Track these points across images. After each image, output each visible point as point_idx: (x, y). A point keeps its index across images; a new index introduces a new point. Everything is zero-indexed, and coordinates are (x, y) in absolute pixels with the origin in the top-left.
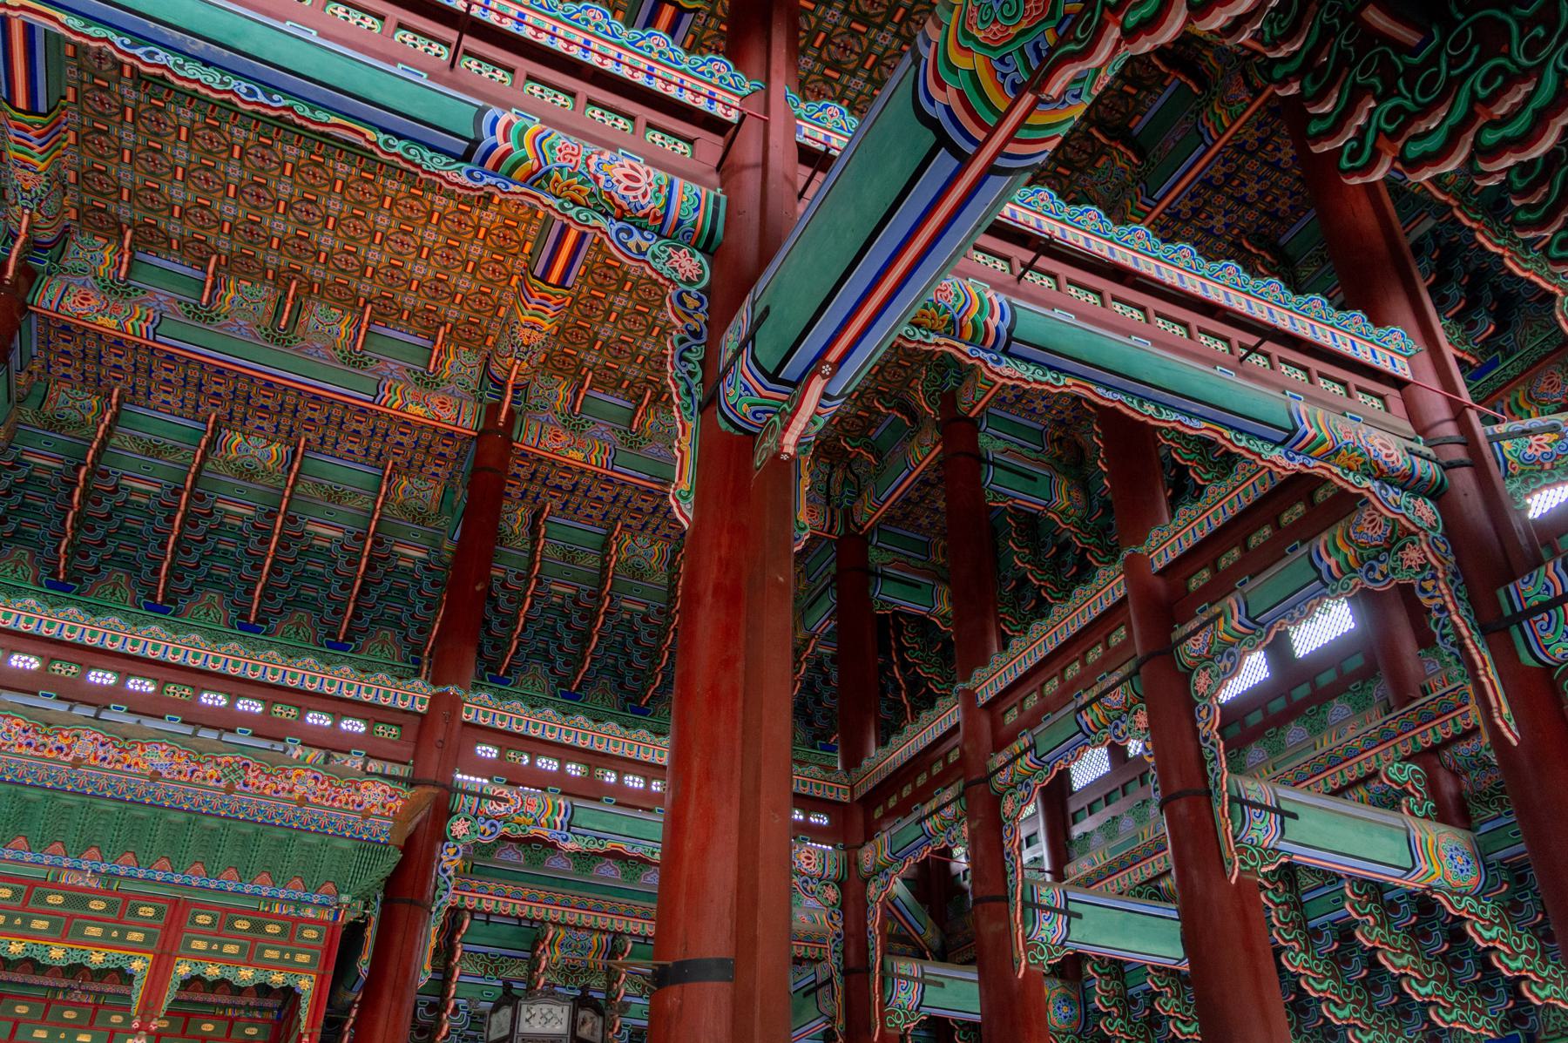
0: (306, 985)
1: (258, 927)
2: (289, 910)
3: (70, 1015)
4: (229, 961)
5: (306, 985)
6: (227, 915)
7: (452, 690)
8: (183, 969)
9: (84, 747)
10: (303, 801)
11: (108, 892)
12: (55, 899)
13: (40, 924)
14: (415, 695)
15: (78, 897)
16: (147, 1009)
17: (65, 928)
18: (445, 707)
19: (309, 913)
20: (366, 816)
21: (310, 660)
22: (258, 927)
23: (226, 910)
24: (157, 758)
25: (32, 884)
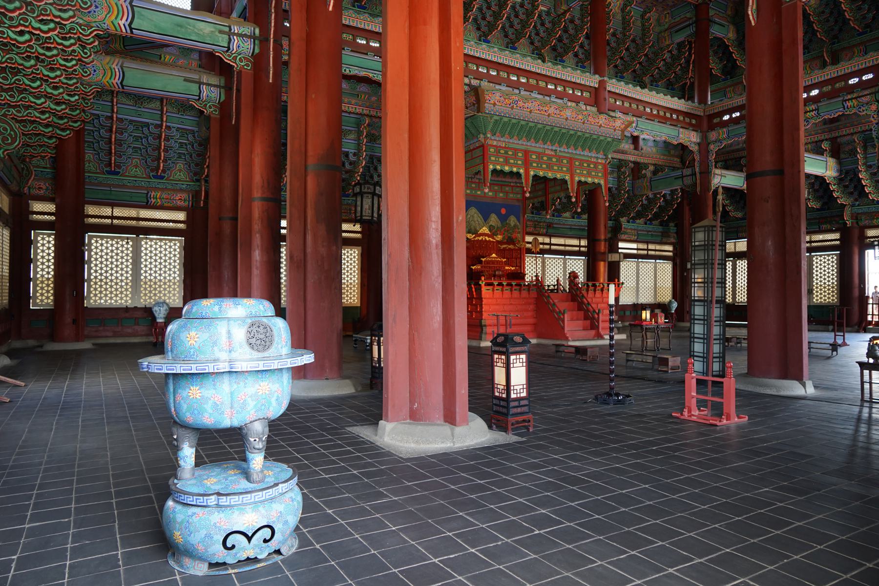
0: (602, 182)
1: (589, 166)
2: (595, 160)
3: (473, 185)
4: (585, 176)
5: (602, 182)
6: (582, 161)
7: (605, 78)
8: (577, 179)
9: (551, 110)
10: (600, 126)
11: (555, 156)
12: (545, 158)
13: (544, 166)
14: (592, 80)
15: (550, 157)
16: (572, 189)
17: (550, 167)
18: (602, 83)
19: (600, 161)
20: (615, 130)
21: (529, 58)
22: (589, 166)
23: (581, 160)
24: (568, 113)
25: (539, 154)
